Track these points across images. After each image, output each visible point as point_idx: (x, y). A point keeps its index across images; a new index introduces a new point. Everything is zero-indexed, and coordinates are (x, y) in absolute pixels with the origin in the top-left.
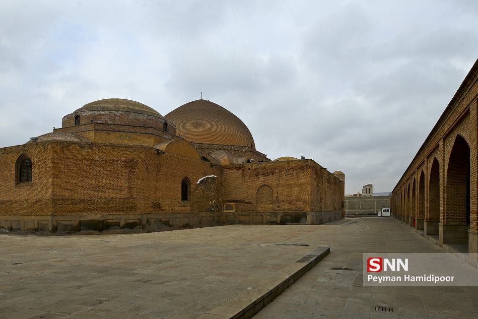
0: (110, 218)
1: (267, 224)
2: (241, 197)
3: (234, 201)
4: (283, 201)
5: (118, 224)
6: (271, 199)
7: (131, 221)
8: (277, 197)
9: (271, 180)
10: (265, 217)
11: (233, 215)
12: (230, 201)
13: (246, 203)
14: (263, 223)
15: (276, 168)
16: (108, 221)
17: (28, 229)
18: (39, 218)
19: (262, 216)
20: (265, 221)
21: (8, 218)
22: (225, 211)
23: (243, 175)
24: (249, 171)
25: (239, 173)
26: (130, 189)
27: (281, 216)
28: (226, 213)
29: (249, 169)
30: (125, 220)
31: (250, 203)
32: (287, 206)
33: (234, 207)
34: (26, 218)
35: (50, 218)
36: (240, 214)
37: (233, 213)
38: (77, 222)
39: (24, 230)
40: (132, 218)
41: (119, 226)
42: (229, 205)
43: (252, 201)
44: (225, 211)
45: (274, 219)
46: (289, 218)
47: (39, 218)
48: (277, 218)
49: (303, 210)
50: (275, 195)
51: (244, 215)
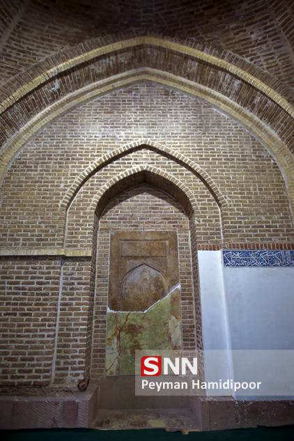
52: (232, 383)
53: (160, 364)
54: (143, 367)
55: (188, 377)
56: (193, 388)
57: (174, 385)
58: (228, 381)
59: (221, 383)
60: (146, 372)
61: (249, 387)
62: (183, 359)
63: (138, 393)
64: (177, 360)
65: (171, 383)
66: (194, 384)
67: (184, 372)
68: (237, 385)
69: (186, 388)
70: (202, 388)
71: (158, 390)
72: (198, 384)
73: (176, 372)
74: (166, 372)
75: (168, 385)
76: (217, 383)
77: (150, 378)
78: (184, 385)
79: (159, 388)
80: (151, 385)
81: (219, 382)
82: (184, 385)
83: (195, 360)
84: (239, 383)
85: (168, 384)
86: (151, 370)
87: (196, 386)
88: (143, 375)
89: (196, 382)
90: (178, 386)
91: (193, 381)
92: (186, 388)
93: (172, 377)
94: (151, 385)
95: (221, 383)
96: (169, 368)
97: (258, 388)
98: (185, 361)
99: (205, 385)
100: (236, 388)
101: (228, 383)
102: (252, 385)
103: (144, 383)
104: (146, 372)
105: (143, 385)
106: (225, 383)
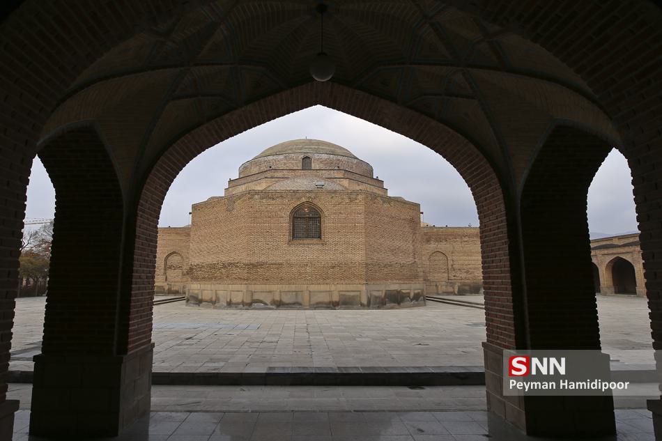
0: (405, 288)
9: (443, 246)
16: (404, 291)
17: (317, 303)
18: (342, 287)
19: (436, 285)
20: (440, 292)
21: (274, 287)
27: (459, 286)
32: (464, 275)
34: (313, 288)
35: (364, 288)
39: (310, 305)
41: (409, 297)
45: (450, 289)
46: (467, 288)
47: (342, 287)
52: (600, 383)
53: (528, 364)
54: (512, 368)
55: (557, 377)
56: (561, 388)
57: (542, 385)
58: (596, 380)
59: (589, 384)
60: (514, 372)
61: (617, 387)
62: (551, 359)
63: (505, 394)
64: (545, 360)
65: (539, 383)
66: (562, 384)
67: (552, 372)
68: (605, 386)
69: (554, 388)
70: (570, 388)
71: (527, 390)
72: (566, 384)
73: (544, 372)
74: (534, 372)
75: (536, 385)
76: (585, 383)
77: (517, 378)
78: (552, 385)
79: (527, 388)
80: (519, 385)
81: (587, 382)
82: (552, 385)
83: (563, 360)
84: (607, 383)
85: (536, 384)
86: (519, 370)
87: (564, 386)
88: (511, 374)
89: (564, 382)
90: (546, 386)
91: (561, 381)
92: (554, 388)
93: (540, 377)
94: (519, 385)
95: (589, 384)
96: (537, 368)
97: (626, 388)
98: (553, 361)
99: (574, 385)
100: (604, 388)
101: (596, 383)
102: (620, 385)
103: (512, 383)
104: (514, 372)
105: (511, 385)
106: (592, 383)
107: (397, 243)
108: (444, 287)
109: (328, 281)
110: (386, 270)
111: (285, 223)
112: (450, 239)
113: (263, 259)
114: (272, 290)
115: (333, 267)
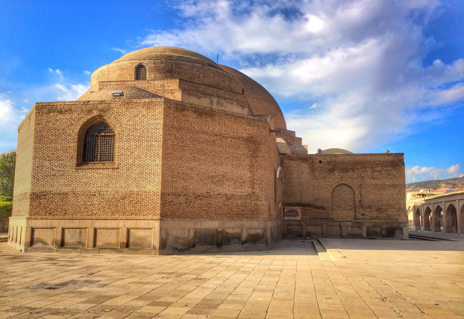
0: (232, 227)
1: (348, 238)
2: (307, 199)
3: (298, 205)
4: (369, 207)
5: (238, 237)
6: (351, 203)
7: (253, 232)
8: (360, 201)
10: (344, 227)
11: (298, 224)
12: (292, 205)
13: (318, 208)
14: (342, 237)
15: (360, 163)
19: (340, 226)
20: (344, 234)
22: (286, 218)
23: (313, 169)
24: (321, 165)
25: (305, 166)
26: (252, 182)
27: (368, 228)
28: (287, 220)
29: (320, 162)
30: (248, 229)
31: (322, 208)
32: (374, 214)
33: (300, 213)
36: (309, 224)
37: (298, 221)
38: (192, 234)
40: (254, 226)
41: (240, 240)
42: (292, 211)
43: (326, 206)
44: (286, 218)
45: (357, 231)
47: (130, 224)
48: (361, 229)
49: (397, 219)
50: (357, 200)
51: (313, 225)
107: (222, 169)
108: (350, 228)
109: (117, 216)
110: (198, 202)
111: (72, 145)
112: (358, 169)
113: (47, 188)
114: (54, 226)
115: (123, 198)
